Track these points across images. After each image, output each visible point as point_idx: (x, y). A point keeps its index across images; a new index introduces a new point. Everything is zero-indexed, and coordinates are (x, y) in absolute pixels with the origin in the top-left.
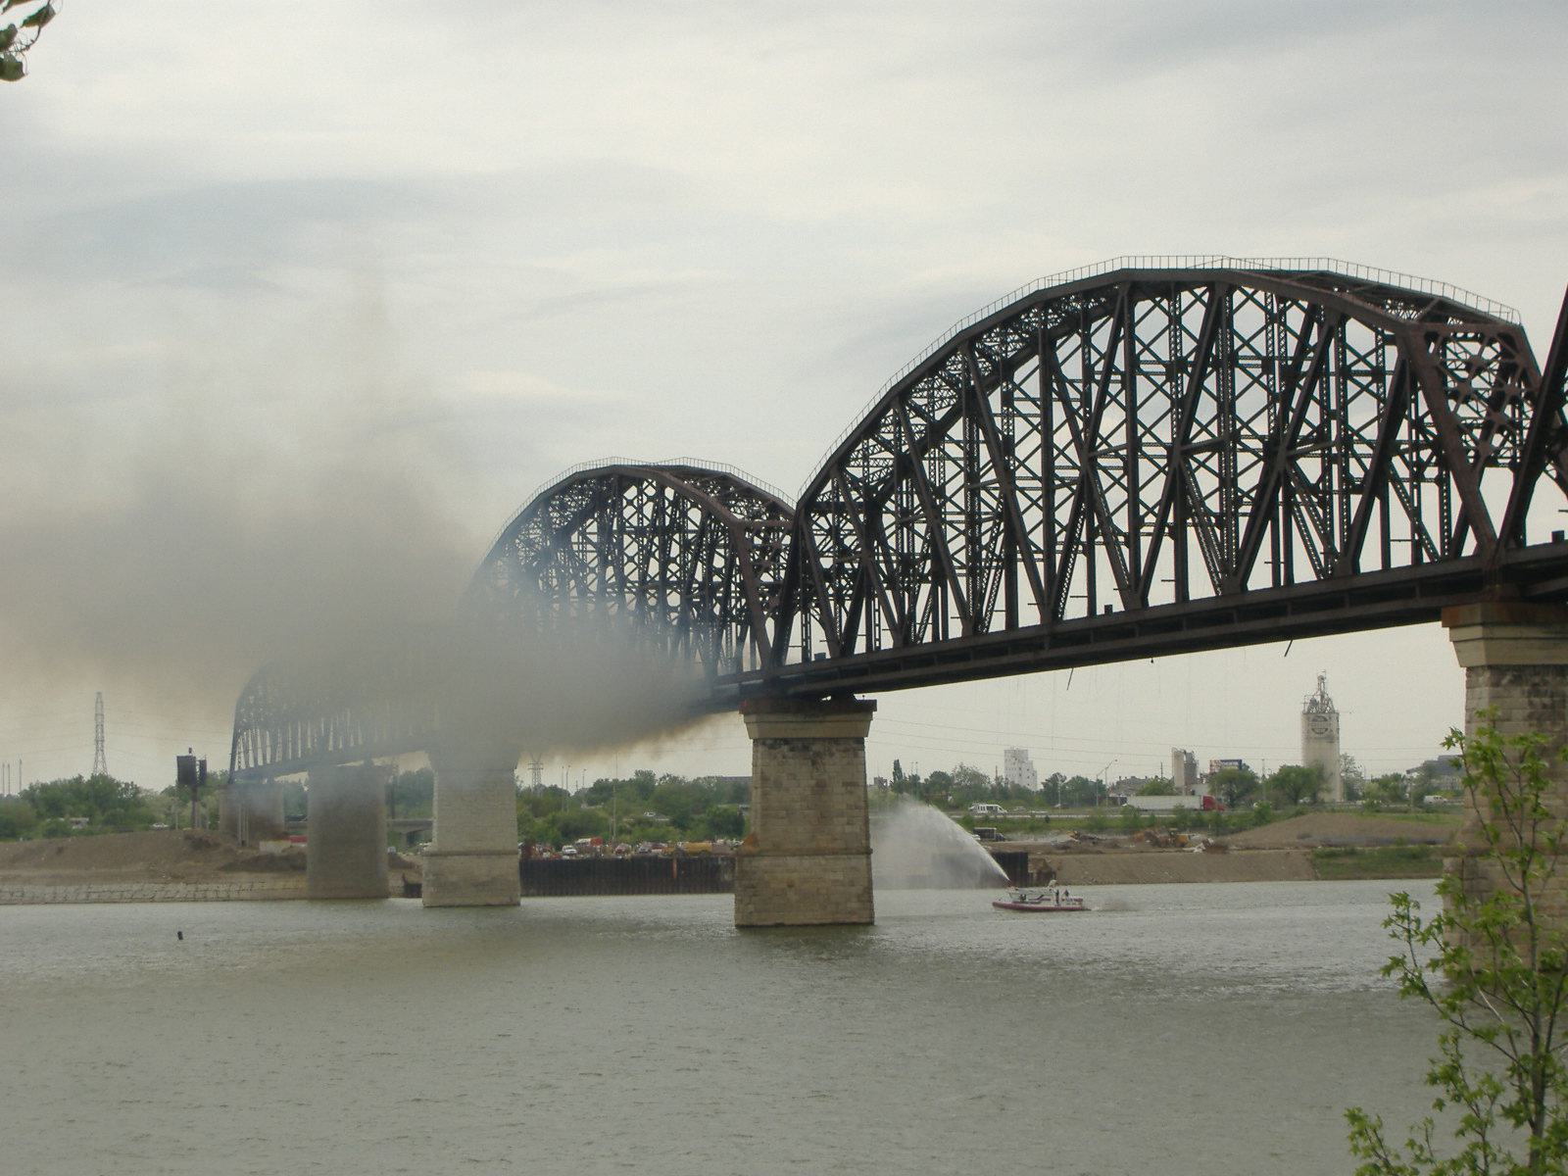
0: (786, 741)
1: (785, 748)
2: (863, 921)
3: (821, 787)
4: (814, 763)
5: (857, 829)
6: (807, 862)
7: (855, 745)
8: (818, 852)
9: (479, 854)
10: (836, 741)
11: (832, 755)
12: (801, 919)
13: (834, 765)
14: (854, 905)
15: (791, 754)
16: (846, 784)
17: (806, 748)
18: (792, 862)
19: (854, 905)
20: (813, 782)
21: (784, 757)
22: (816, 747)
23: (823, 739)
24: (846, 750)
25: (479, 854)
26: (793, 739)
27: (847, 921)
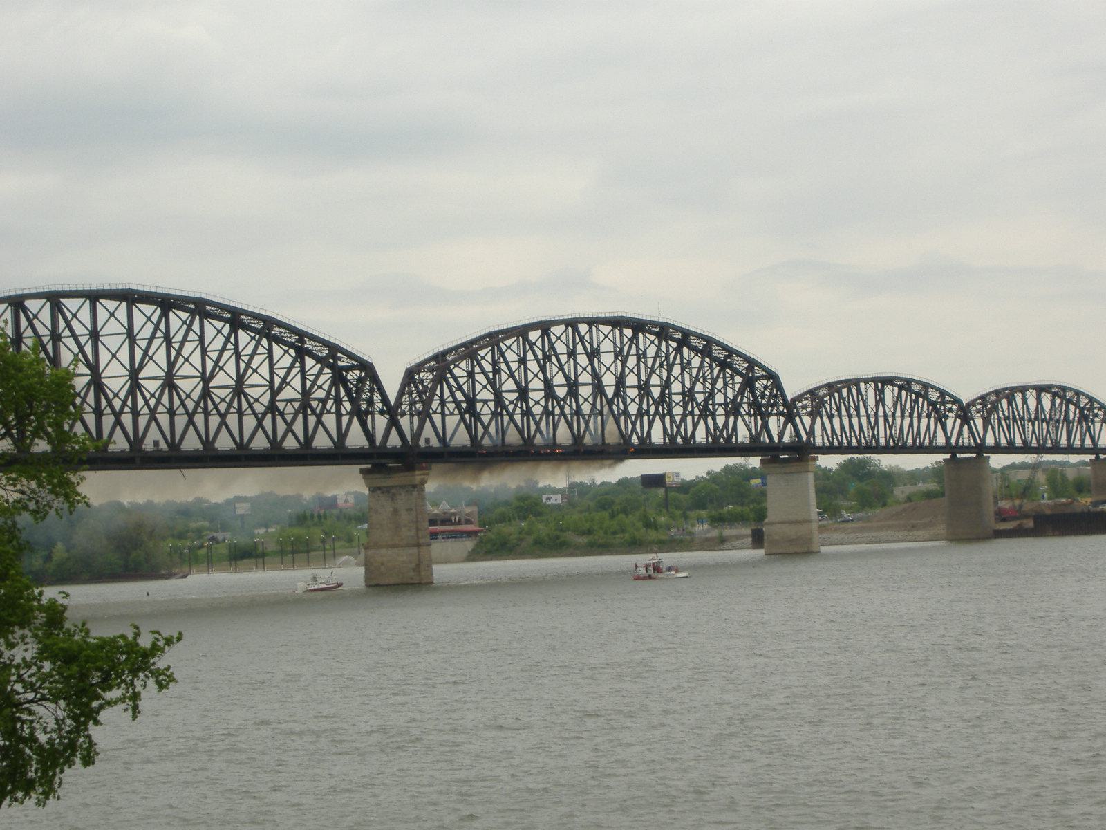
0: (379, 488)
1: (379, 492)
2: (416, 582)
3: (396, 511)
4: (393, 499)
5: (413, 533)
6: (390, 552)
7: (412, 489)
8: (394, 546)
9: (790, 522)
10: (401, 487)
11: (400, 494)
12: (387, 582)
13: (402, 500)
14: (412, 574)
15: (382, 495)
16: (407, 510)
17: (388, 492)
18: (383, 551)
19: (412, 574)
20: (391, 509)
21: (379, 497)
22: (393, 491)
23: (397, 486)
24: (407, 491)
25: (790, 522)
26: (384, 487)
27: (409, 582)
